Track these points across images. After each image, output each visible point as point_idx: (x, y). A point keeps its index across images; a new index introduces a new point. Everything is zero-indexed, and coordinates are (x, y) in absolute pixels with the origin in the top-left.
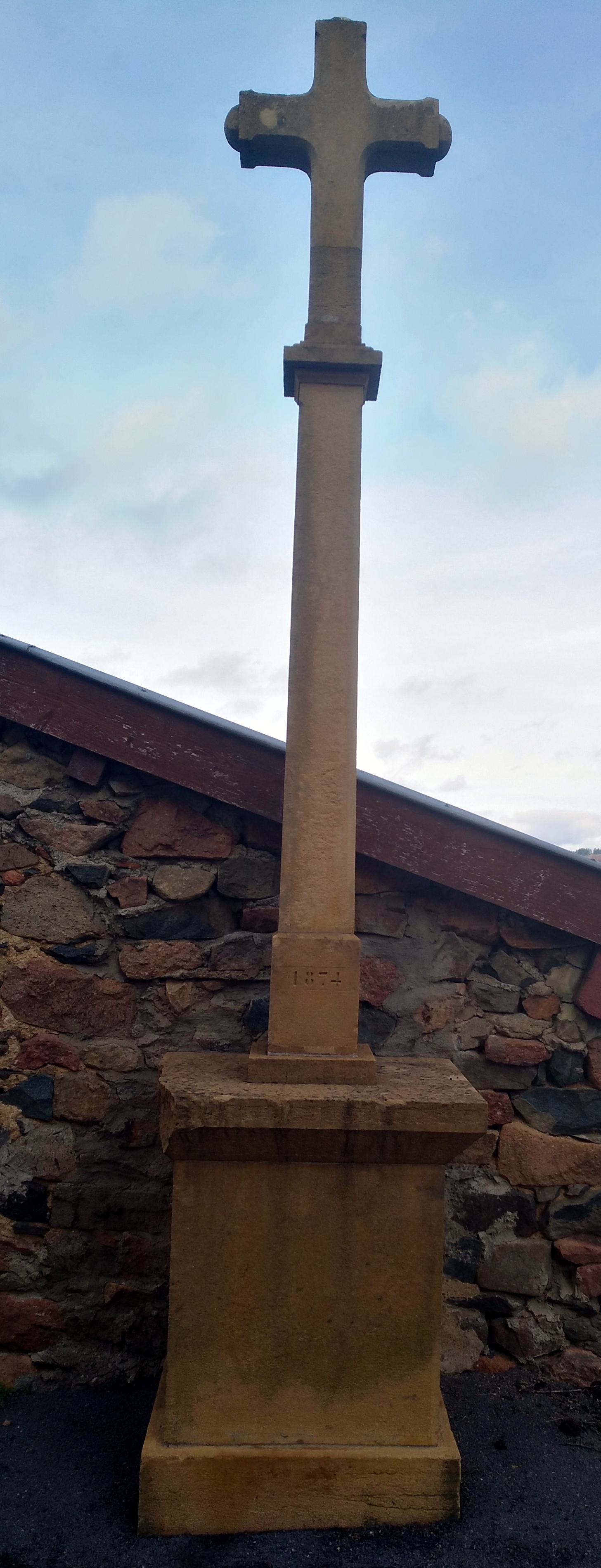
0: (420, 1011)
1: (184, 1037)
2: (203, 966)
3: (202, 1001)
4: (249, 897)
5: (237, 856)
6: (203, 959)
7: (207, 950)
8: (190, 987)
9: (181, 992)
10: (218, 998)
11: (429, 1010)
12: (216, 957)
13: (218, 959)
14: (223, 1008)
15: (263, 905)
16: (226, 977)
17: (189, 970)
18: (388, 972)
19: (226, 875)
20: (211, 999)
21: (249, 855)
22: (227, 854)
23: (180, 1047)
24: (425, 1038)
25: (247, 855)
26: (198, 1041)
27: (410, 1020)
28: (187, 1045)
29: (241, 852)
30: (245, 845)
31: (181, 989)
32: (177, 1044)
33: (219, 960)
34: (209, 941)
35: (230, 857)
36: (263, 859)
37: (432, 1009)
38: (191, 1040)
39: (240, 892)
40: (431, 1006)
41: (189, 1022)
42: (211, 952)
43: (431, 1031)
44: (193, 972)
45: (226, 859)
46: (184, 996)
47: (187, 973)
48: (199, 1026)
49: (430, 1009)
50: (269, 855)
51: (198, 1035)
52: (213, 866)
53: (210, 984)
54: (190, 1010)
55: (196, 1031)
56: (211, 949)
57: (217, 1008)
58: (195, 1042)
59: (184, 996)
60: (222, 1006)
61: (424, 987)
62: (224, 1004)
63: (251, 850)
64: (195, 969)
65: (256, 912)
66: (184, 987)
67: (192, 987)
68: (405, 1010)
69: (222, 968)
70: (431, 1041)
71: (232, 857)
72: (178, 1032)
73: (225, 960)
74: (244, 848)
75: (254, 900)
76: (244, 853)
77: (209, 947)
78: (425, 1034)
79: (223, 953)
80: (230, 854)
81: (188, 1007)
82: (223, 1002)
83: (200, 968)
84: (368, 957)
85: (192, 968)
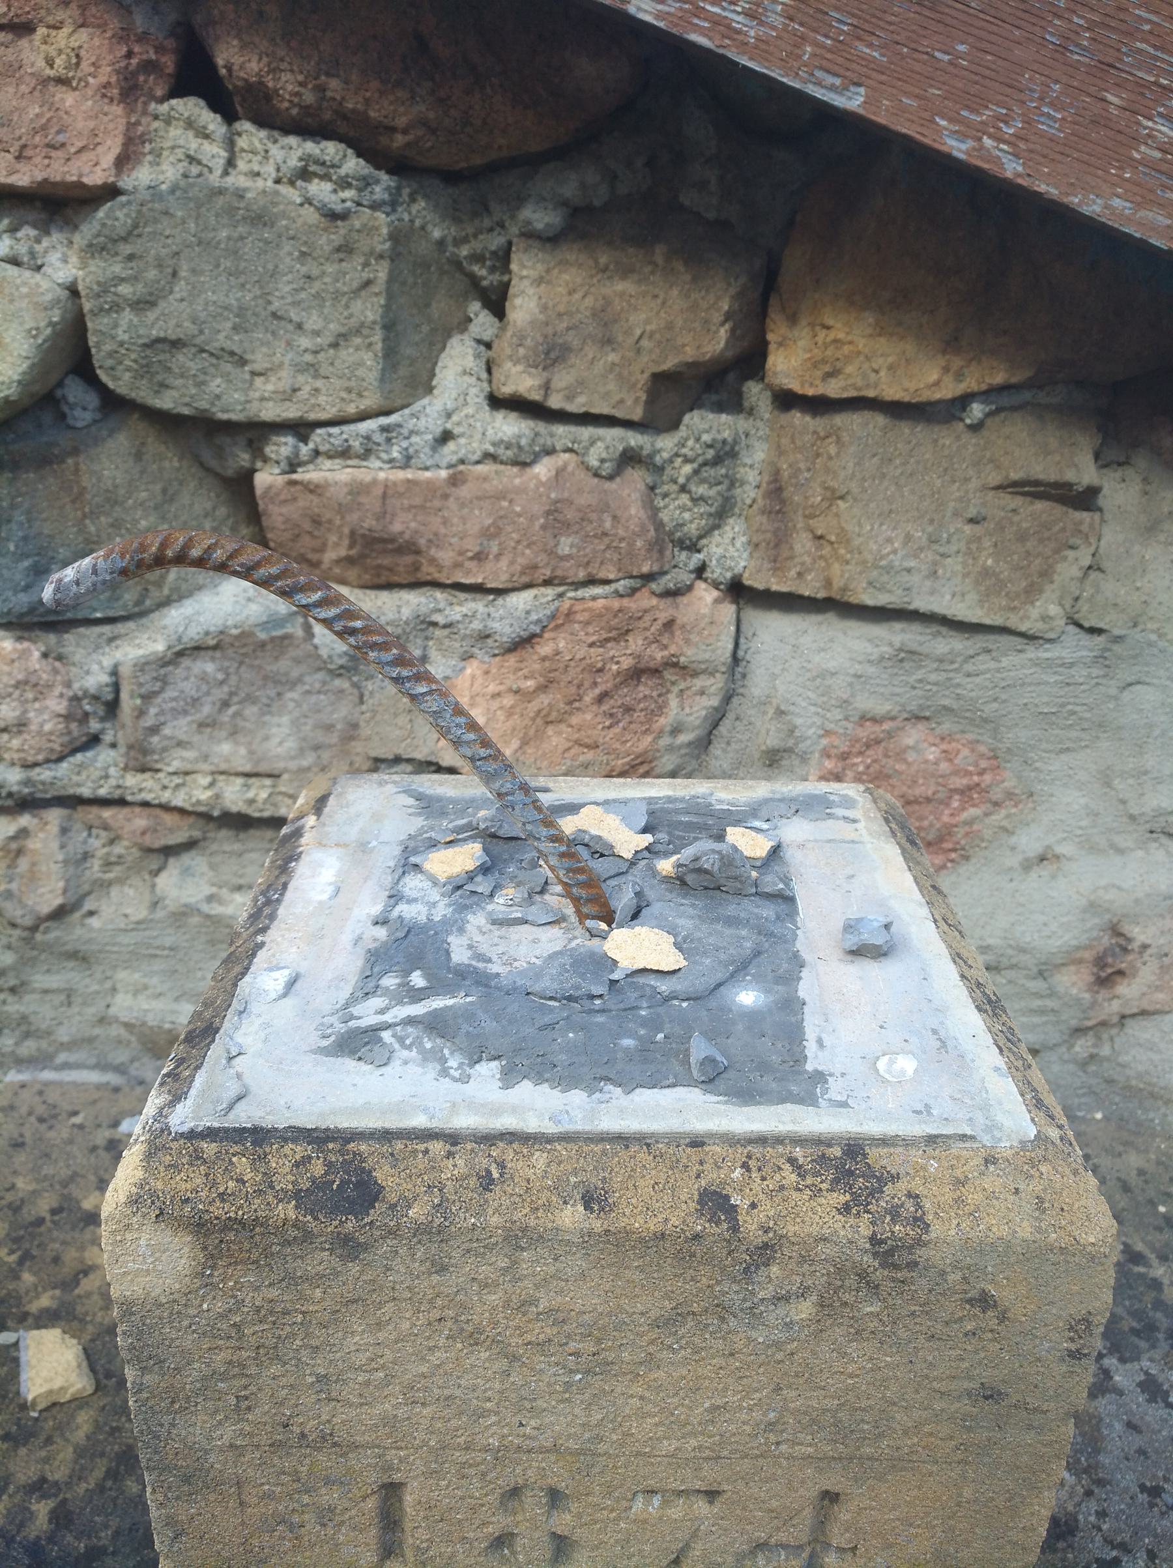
0: (1088, 955)
1: (75, 1009)
2: (94, 740)
3: (120, 881)
4: (270, 412)
5: (169, 172)
6: (86, 715)
7: (96, 679)
8: (54, 828)
9: (20, 852)
10: (186, 872)
11: (1125, 950)
12: (141, 713)
13: (149, 721)
14: (208, 917)
15: (344, 453)
16: (199, 802)
17: (28, 766)
18: (960, 782)
19: (124, 289)
20: (156, 873)
21: (242, 165)
22: (108, 159)
23: (69, 1046)
24: (1082, 1047)
25: (231, 163)
26: (128, 1026)
27: (1037, 985)
28: (90, 1040)
29: (193, 144)
30: (214, 107)
31: (13, 838)
32: (49, 1033)
33: (154, 730)
34: (106, 629)
35: (126, 183)
36: (320, 189)
37: (1145, 947)
38: (102, 1020)
39: (216, 384)
40: (1139, 934)
41: (79, 957)
42: (116, 687)
43: (1115, 1019)
44: (44, 774)
45: (111, 192)
46: (34, 864)
47: (19, 783)
48: (122, 975)
49: (1135, 945)
50: (353, 165)
51: (124, 1005)
52: (56, 237)
53: (140, 821)
54: (77, 915)
55: (114, 990)
56: (114, 673)
57: (184, 914)
58: (115, 1031)
59: (34, 864)
60: (205, 908)
61: (1121, 851)
62: (210, 898)
63: (251, 135)
64: (61, 759)
65: (312, 489)
66: (23, 833)
67: (64, 831)
68: (1023, 951)
69: (176, 765)
70: (1106, 1051)
71: (141, 176)
72: (46, 992)
73: (179, 728)
74: (212, 121)
75: (301, 429)
76: (214, 153)
77: (107, 662)
78: (1079, 1031)
79: (170, 693)
80: (123, 161)
81: (60, 913)
82: (208, 890)
83: (79, 757)
84: (865, 718)
85: (40, 758)
